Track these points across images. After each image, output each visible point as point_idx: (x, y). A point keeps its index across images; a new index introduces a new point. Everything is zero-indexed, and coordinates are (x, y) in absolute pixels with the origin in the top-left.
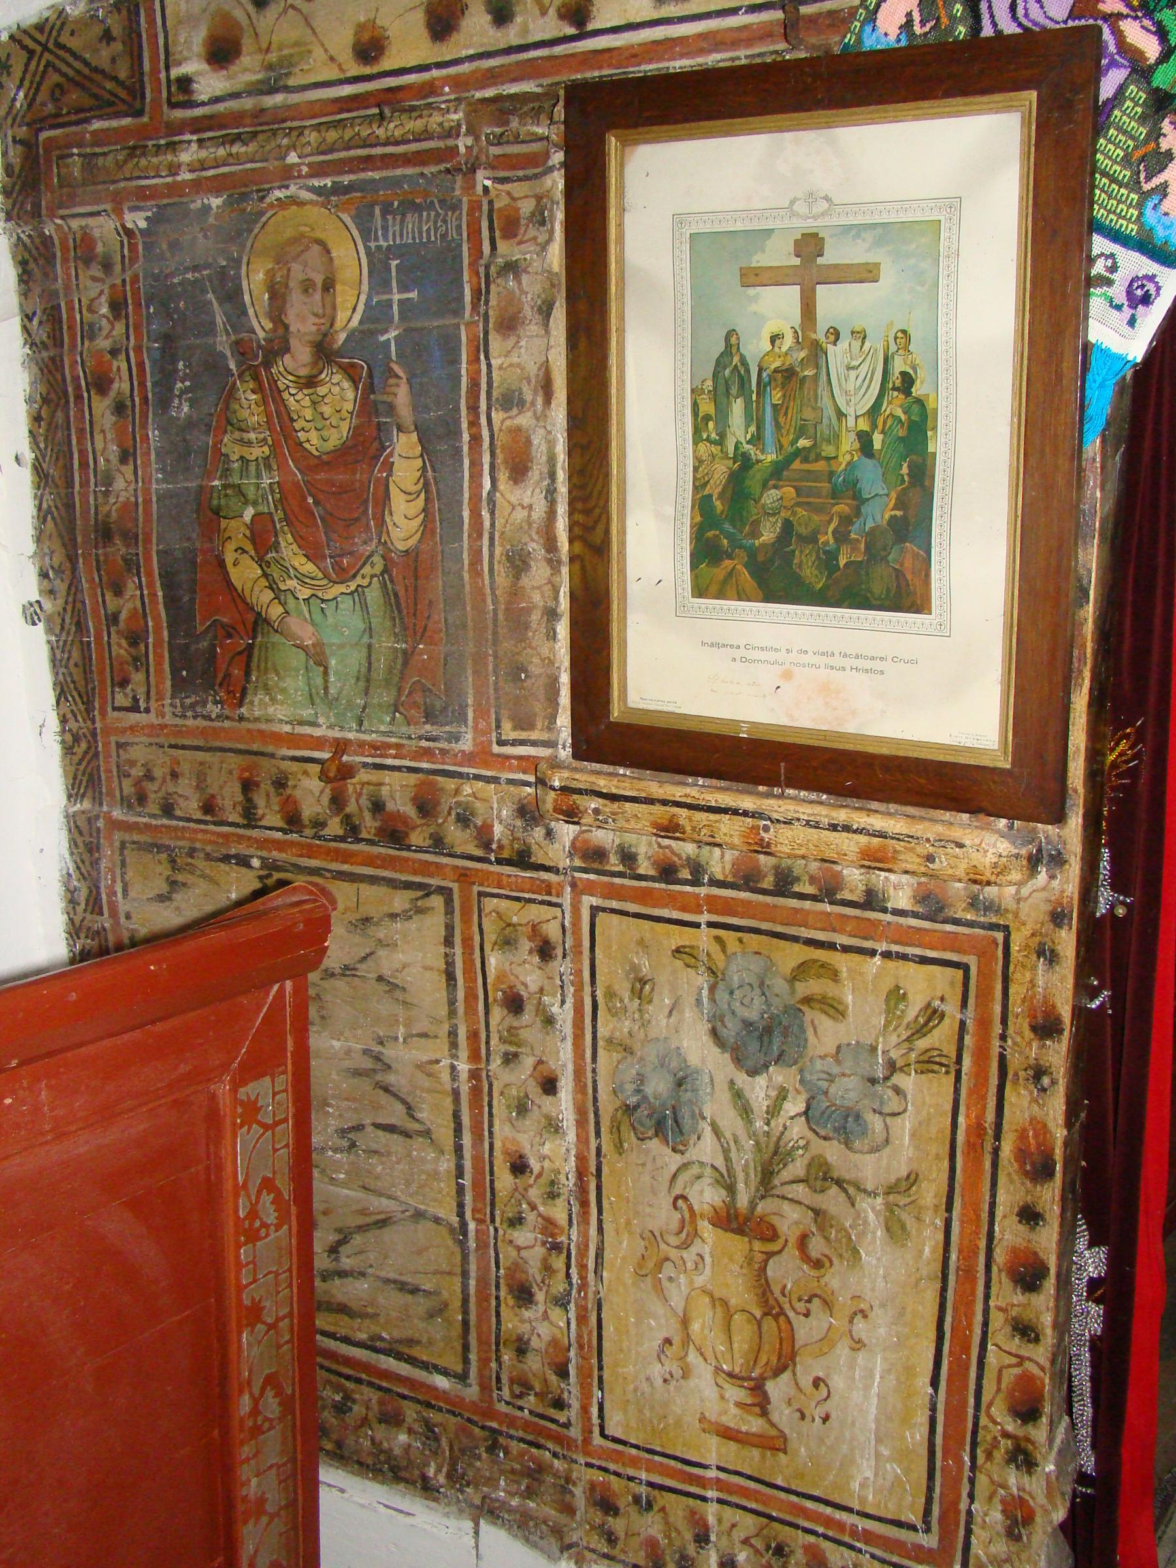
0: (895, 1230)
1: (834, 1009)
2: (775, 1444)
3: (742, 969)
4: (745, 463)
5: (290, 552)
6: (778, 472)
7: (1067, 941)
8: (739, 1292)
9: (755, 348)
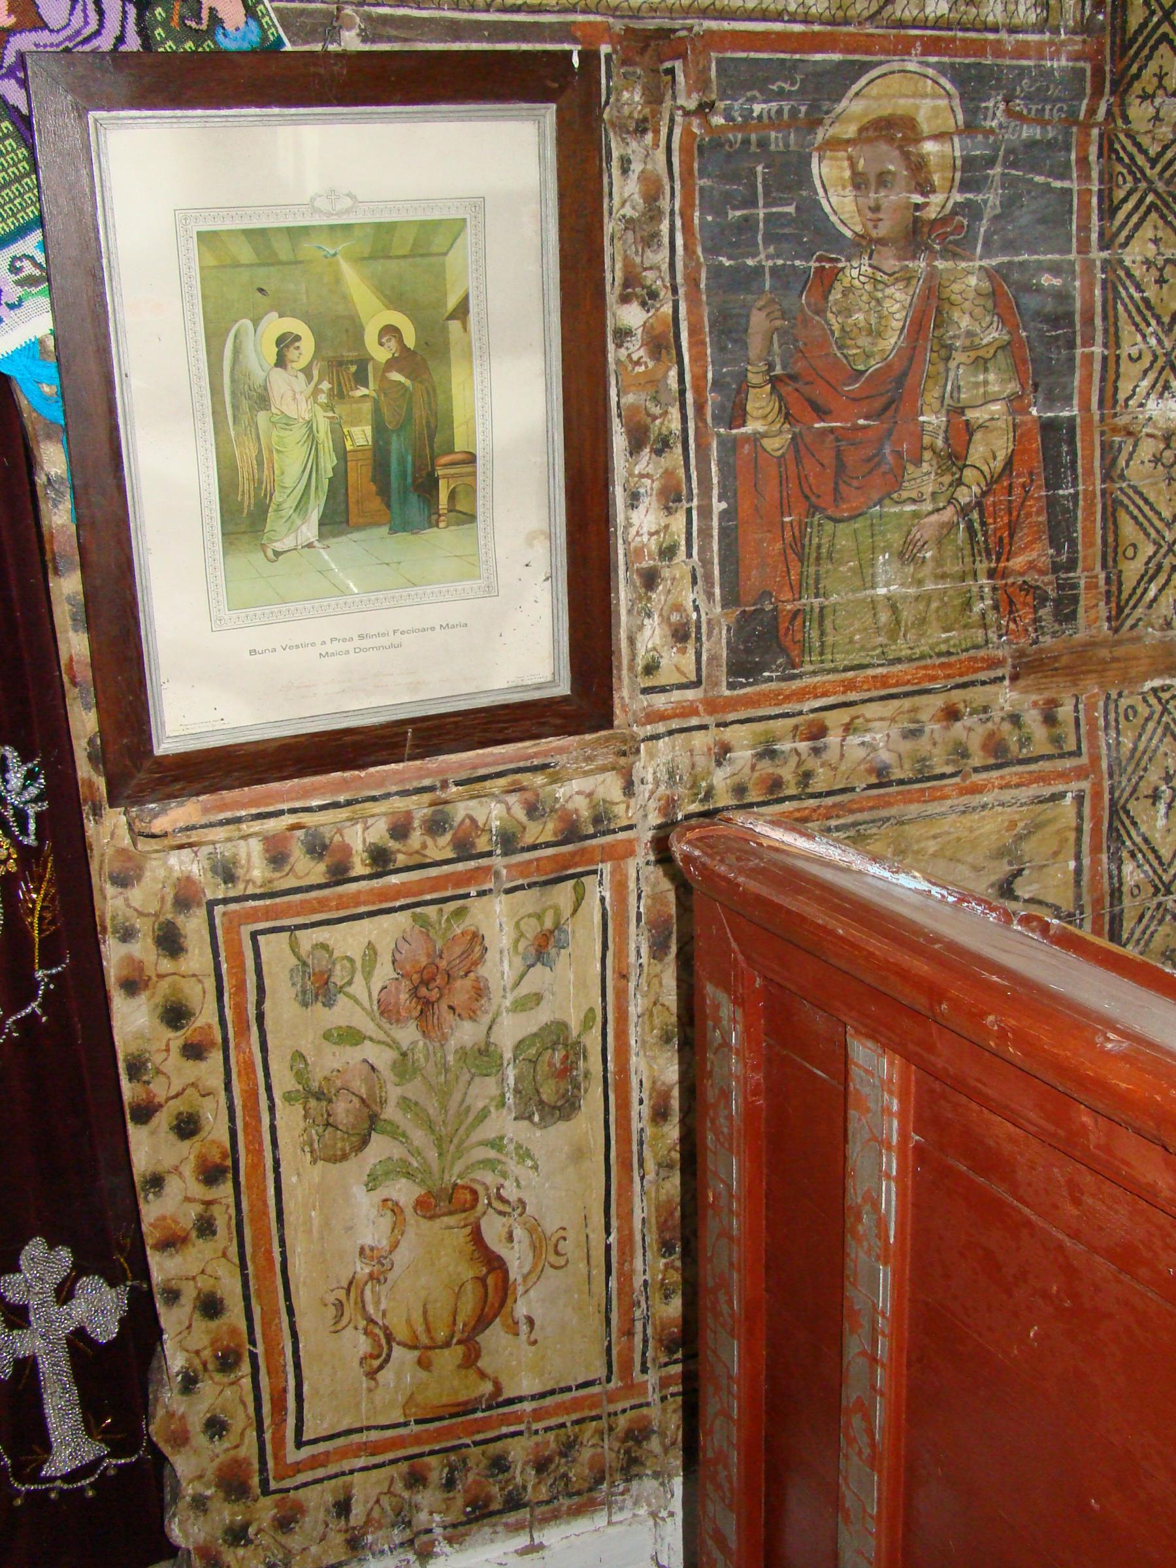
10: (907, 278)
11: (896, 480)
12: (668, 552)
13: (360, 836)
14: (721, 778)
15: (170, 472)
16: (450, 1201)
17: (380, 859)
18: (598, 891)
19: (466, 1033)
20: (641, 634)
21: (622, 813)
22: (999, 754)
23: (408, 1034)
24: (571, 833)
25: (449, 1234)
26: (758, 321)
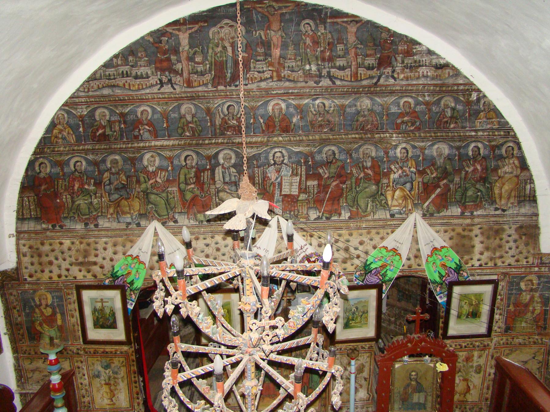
0: (123, 381)
1: (113, 363)
2: (114, 404)
3: (103, 361)
4: (98, 317)
5: (44, 325)
6: (101, 318)
7: (134, 354)
8: (108, 391)
9: (98, 307)
10: (530, 294)
11: (526, 314)
12: (499, 320)
13: (463, 345)
14: (501, 342)
15: (454, 312)
16: (466, 380)
17: (465, 347)
18: (487, 352)
19: (471, 364)
20: (495, 328)
21: (490, 345)
22: (535, 343)
23: (465, 363)
24: (485, 346)
25: (465, 383)
26: (512, 298)
